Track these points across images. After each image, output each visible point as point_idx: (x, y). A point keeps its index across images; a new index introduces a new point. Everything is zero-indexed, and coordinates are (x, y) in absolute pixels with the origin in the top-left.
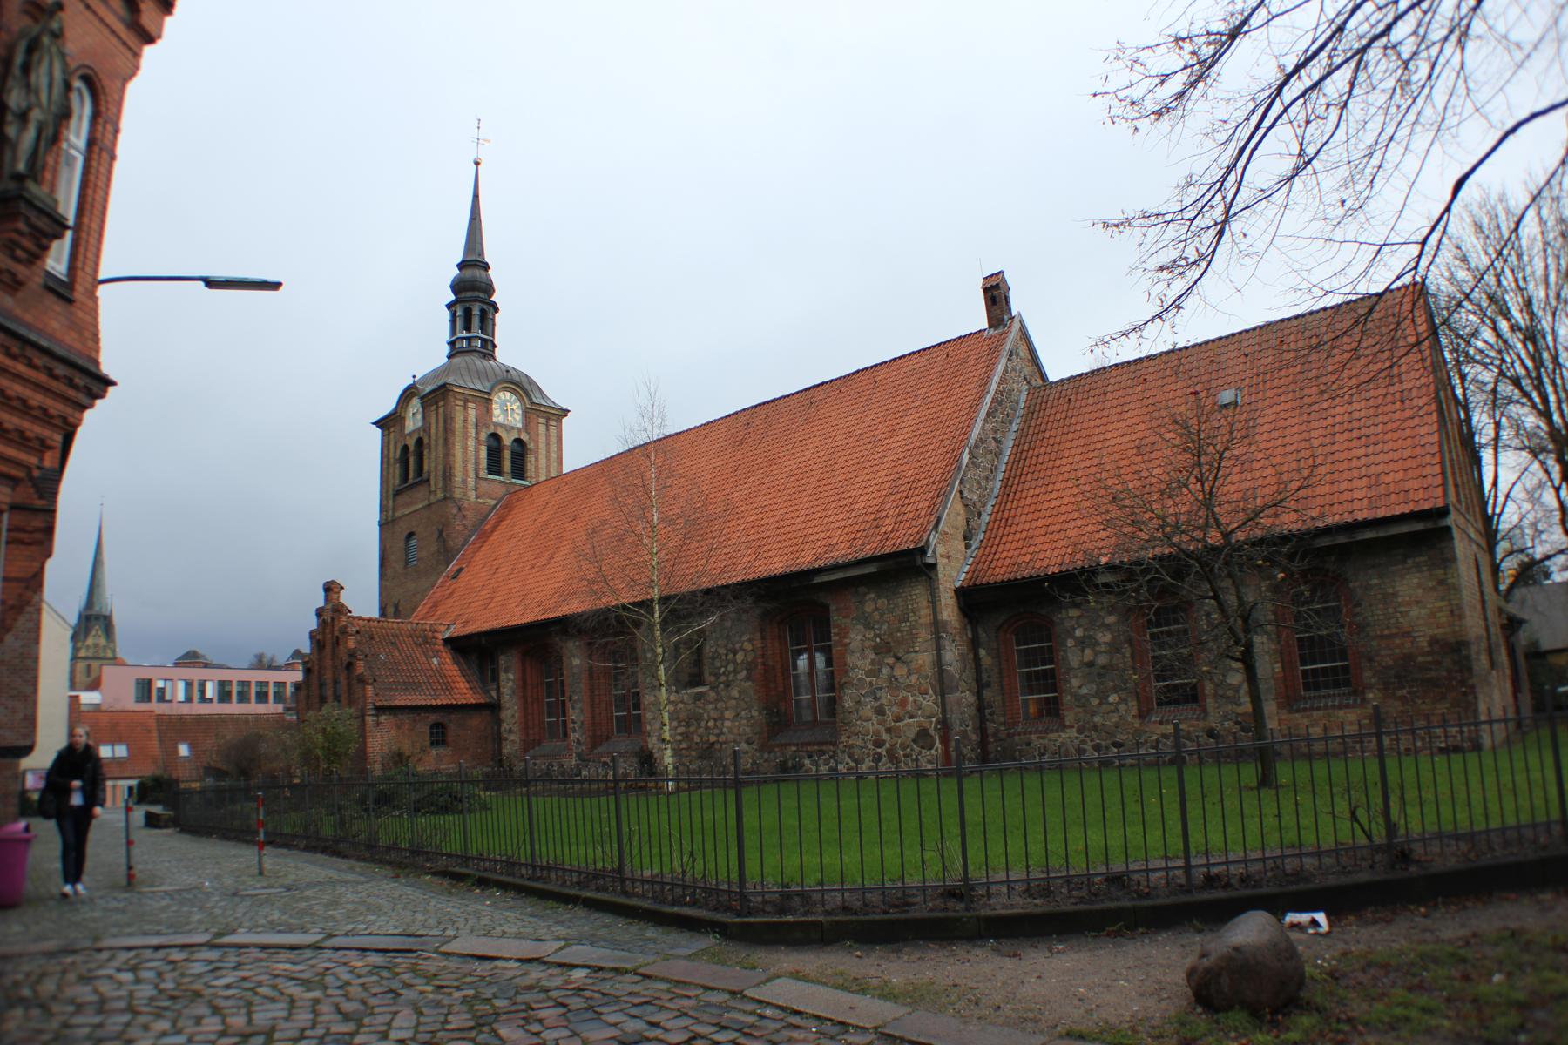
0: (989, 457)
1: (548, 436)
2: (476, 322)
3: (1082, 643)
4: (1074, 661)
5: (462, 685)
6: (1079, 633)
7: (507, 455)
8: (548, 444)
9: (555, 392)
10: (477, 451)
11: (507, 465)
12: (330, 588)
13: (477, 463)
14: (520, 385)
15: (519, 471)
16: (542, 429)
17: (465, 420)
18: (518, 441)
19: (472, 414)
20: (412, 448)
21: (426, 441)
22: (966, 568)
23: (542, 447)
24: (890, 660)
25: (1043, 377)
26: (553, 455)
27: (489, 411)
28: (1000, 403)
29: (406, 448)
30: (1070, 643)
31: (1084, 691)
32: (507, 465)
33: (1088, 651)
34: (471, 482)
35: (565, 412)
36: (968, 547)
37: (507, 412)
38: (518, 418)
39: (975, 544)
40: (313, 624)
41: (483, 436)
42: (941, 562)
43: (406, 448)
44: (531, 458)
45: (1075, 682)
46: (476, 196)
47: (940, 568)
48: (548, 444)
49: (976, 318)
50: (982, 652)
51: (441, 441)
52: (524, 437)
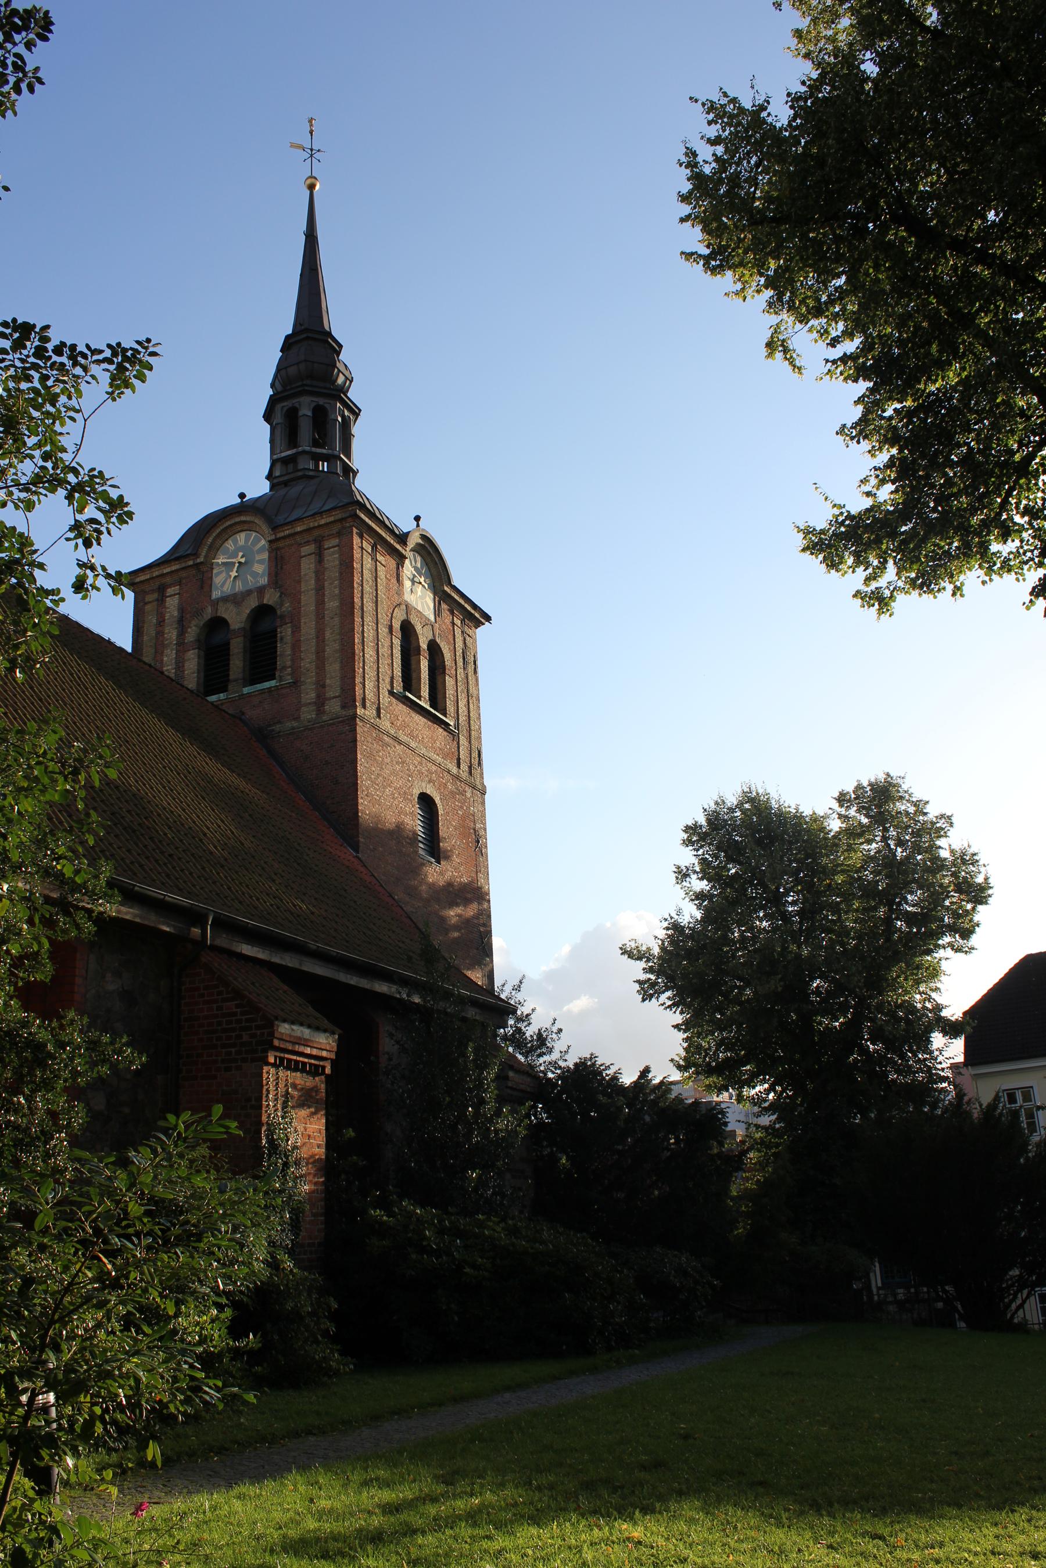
1: (319, 575)
7: (237, 647)
8: (320, 589)
11: (237, 665)
16: (308, 566)
17: (161, 622)
18: (263, 612)
23: (308, 601)
26: (332, 604)
32: (237, 665)
44: (286, 632)
48: (320, 589)
52: (270, 598)
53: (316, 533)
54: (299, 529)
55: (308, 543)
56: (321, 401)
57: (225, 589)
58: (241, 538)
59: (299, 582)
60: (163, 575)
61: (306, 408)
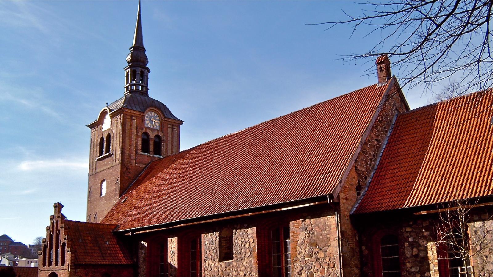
0: (373, 149)
1: (172, 134)
2: (138, 76)
3: (412, 245)
4: (408, 254)
5: (121, 255)
6: (410, 240)
7: (152, 143)
8: (172, 138)
9: (177, 113)
10: (137, 140)
11: (151, 148)
12: (58, 207)
13: (136, 147)
14: (161, 109)
15: (157, 151)
16: (170, 130)
17: (131, 126)
18: (157, 136)
19: (134, 122)
20: (105, 139)
21: (112, 135)
22: (356, 206)
23: (170, 139)
24: (317, 250)
25: (407, 108)
27: (143, 121)
28: (381, 122)
29: (102, 139)
30: (406, 245)
31: (413, 270)
32: (151, 148)
33: (415, 249)
34: (133, 156)
35: (181, 122)
36: (359, 194)
37: (152, 121)
38: (158, 125)
39: (362, 193)
40: (48, 223)
41: (140, 134)
42: (342, 201)
43: (102, 139)
44: (164, 145)
45: (408, 265)
46: (140, 15)
47: (342, 205)
48: (172, 138)
49: (372, 80)
50: (364, 248)
51: (118, 136)
52: (160, 134)
53: (172, 123)
54: (170, 121)
55: (170, 124)
56: (143, 70)
57: (148, 125)
58: (153, 113)
59: (168, 134)
60: (133, 113)
61: (139, 71)
